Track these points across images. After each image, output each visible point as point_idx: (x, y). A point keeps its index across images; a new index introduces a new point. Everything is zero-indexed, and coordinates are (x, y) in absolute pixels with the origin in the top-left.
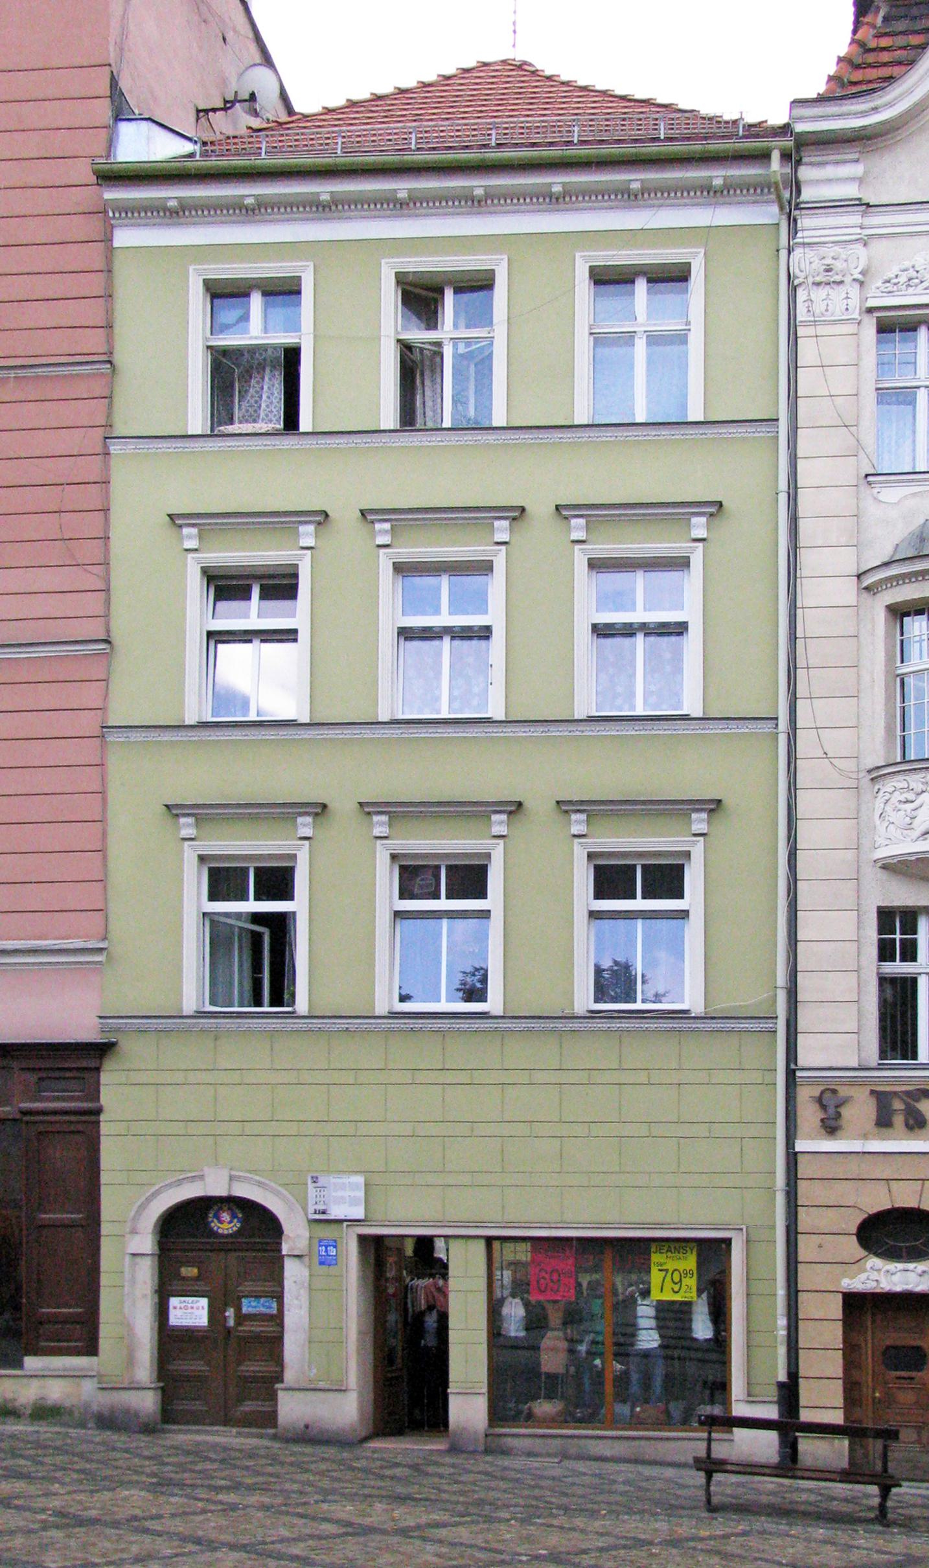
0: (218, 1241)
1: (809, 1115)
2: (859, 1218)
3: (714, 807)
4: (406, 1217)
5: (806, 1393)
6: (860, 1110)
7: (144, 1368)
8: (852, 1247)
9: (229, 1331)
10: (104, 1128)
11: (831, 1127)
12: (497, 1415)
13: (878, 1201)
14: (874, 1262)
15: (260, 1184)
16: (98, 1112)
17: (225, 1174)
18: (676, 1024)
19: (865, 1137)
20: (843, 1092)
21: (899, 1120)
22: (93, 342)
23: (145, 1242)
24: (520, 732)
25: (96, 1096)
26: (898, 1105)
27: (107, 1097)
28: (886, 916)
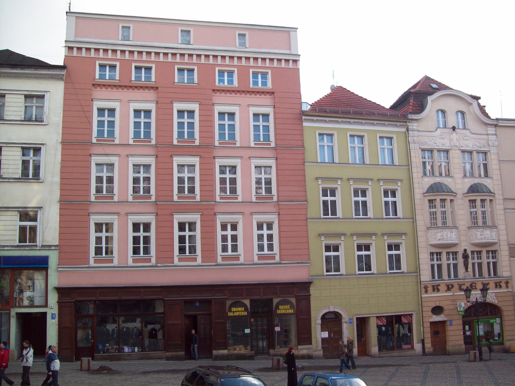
0: (332, 320)
1: (423, 290)
2: (431, 308)
3: (405, 234)
4: (363, 313)
5: (426, 341)
6: (430, 289)
7: (320, 347)
8: (430, 313)
9: (332, 338)
10: (311, 299)
11: (426, 292)
12: (380, 350)
13: (433, 305)
14: (434, 316)
15: (340, 309)
16: (310, 295)
17: (333, 307)
18: (402, 275)
19: (431, 294)
20: (428, 285)
21: (436, 290)
22: (300, 143)
23: (319, 321)
24: (376, 220)
25: (309, 292)
26: (435, 287)
27: (312, 292)
28: (432, 254)
